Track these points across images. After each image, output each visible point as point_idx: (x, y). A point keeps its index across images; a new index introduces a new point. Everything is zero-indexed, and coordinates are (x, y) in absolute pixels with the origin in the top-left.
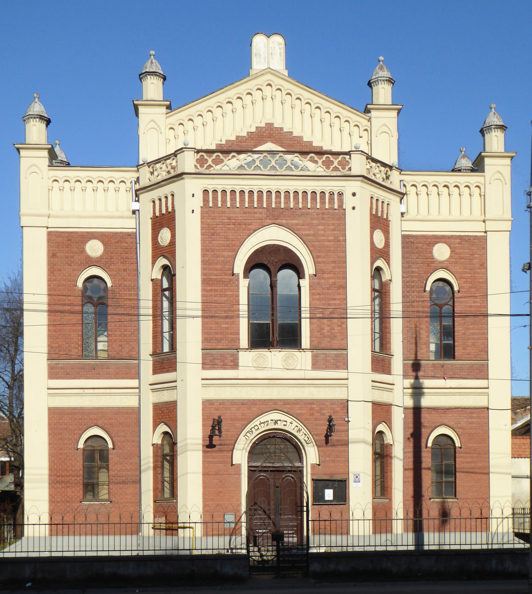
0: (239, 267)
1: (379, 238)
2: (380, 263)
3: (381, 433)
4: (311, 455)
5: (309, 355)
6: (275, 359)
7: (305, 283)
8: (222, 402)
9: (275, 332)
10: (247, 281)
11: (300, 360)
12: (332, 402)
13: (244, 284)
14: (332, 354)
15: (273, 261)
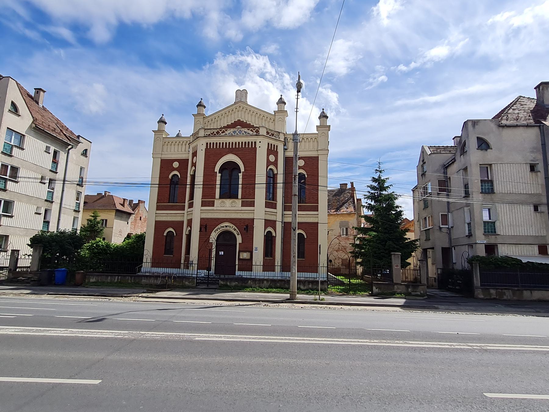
0: (217, 169)
1: (272, 158)
2: (271, 167)
3: (269, 232)
4: (239, 239)
5: (240, 201)
6: (228, 202)
7: (240, 175)
8: (208, 219)
9: (229, 193)
10: (220, 175)
11: (238, 203)
12: (248, 219)
13: (219, 175)
14: (249, 202)
15: (230, 167)
